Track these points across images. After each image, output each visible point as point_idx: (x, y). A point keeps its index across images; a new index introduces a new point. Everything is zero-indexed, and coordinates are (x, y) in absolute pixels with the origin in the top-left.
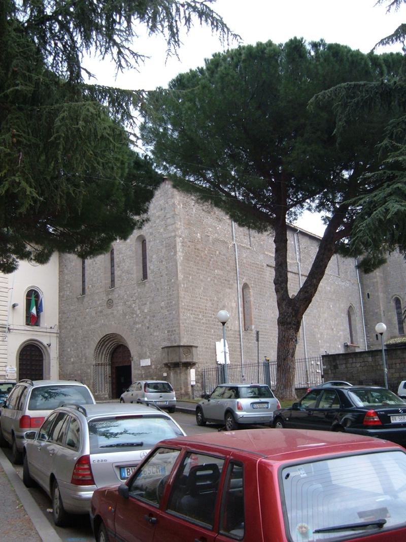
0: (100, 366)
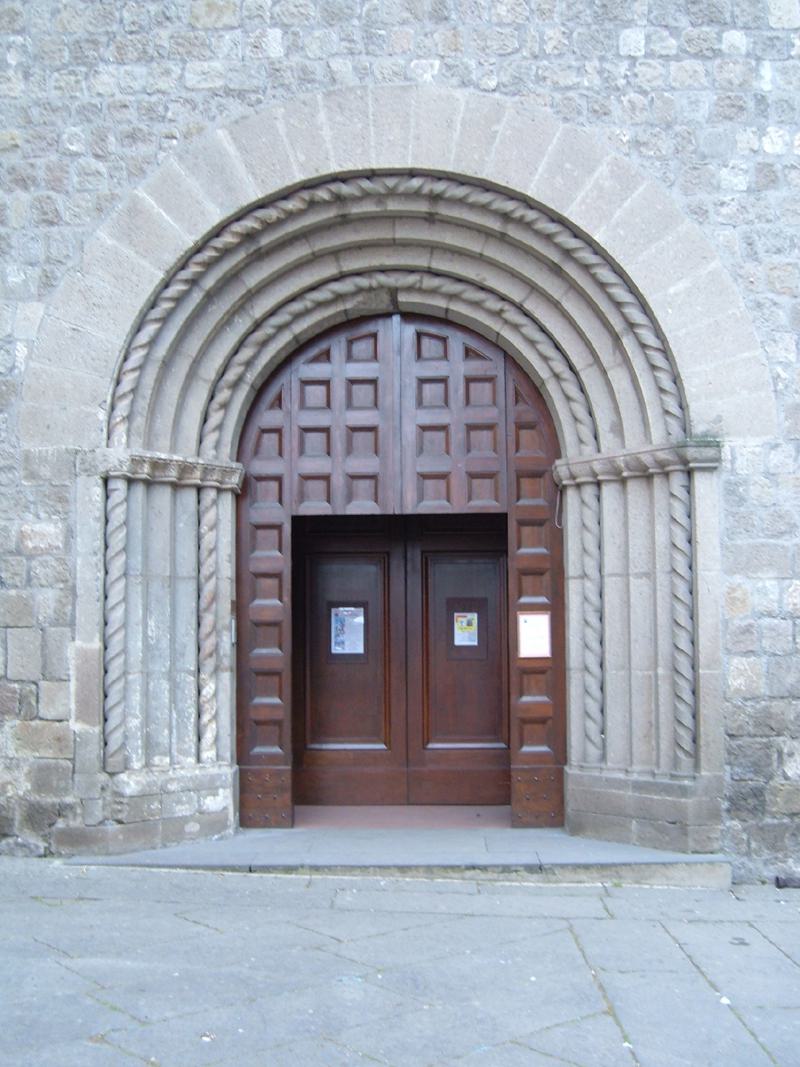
0: (163, 496)
